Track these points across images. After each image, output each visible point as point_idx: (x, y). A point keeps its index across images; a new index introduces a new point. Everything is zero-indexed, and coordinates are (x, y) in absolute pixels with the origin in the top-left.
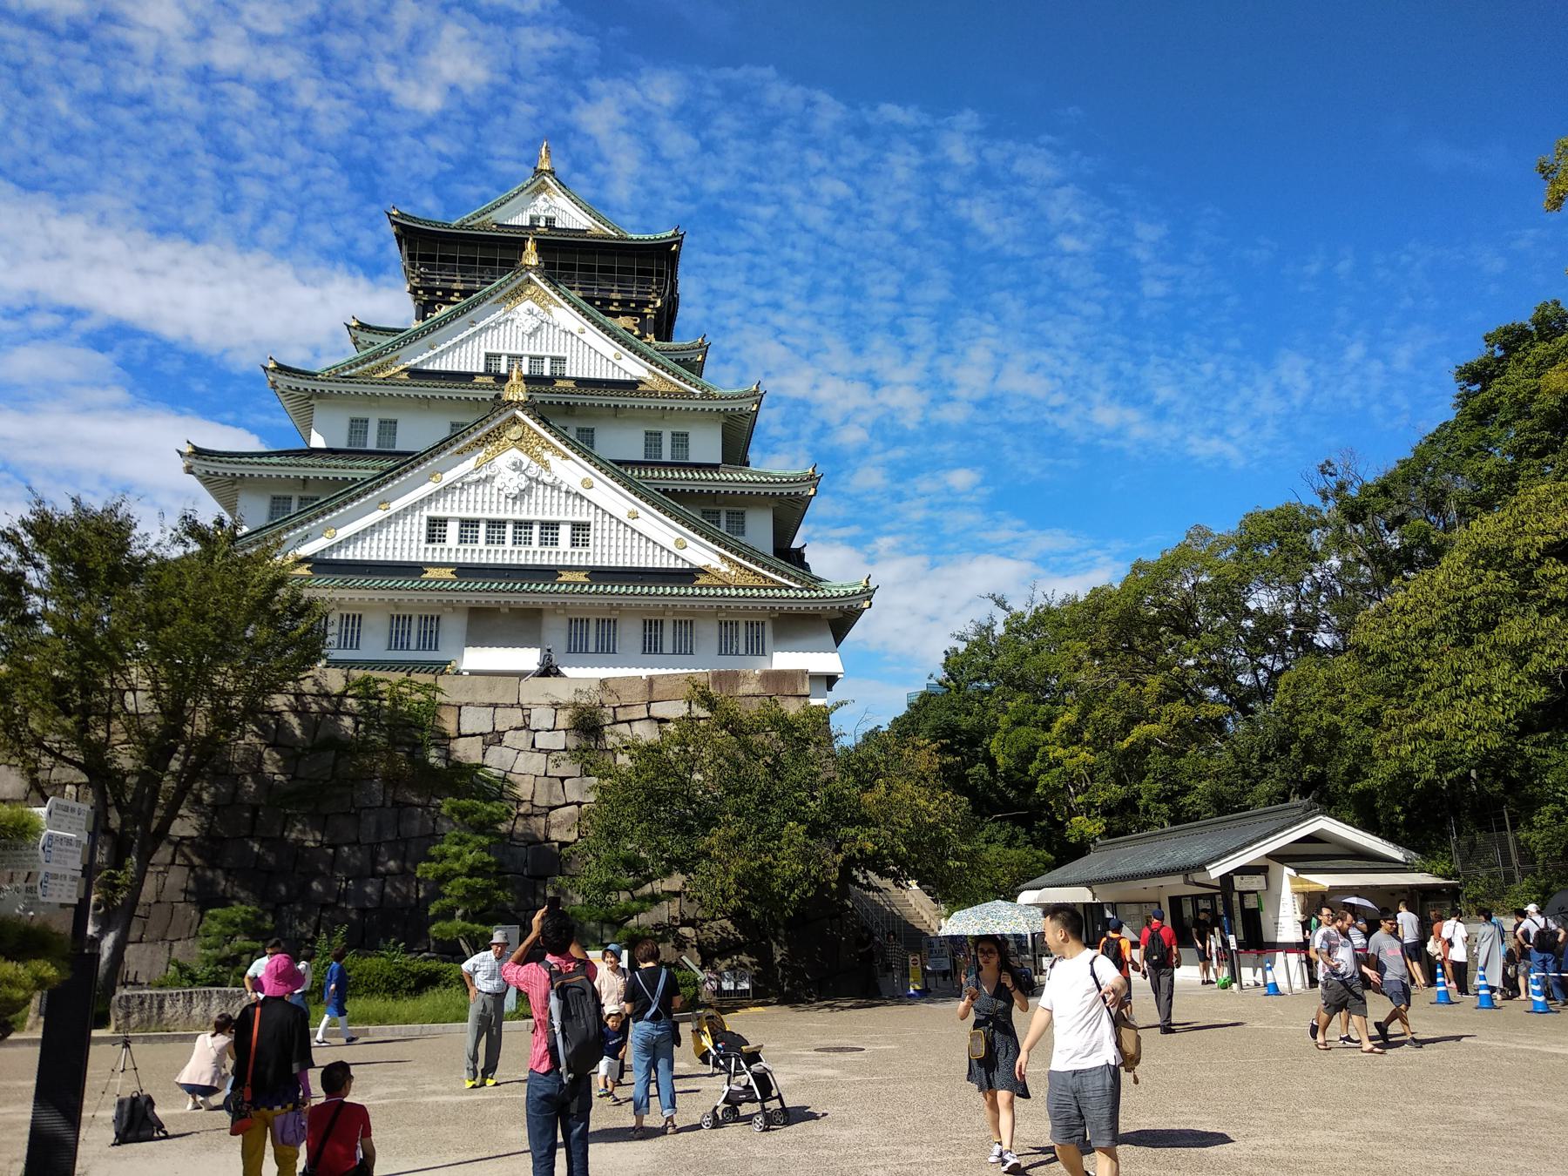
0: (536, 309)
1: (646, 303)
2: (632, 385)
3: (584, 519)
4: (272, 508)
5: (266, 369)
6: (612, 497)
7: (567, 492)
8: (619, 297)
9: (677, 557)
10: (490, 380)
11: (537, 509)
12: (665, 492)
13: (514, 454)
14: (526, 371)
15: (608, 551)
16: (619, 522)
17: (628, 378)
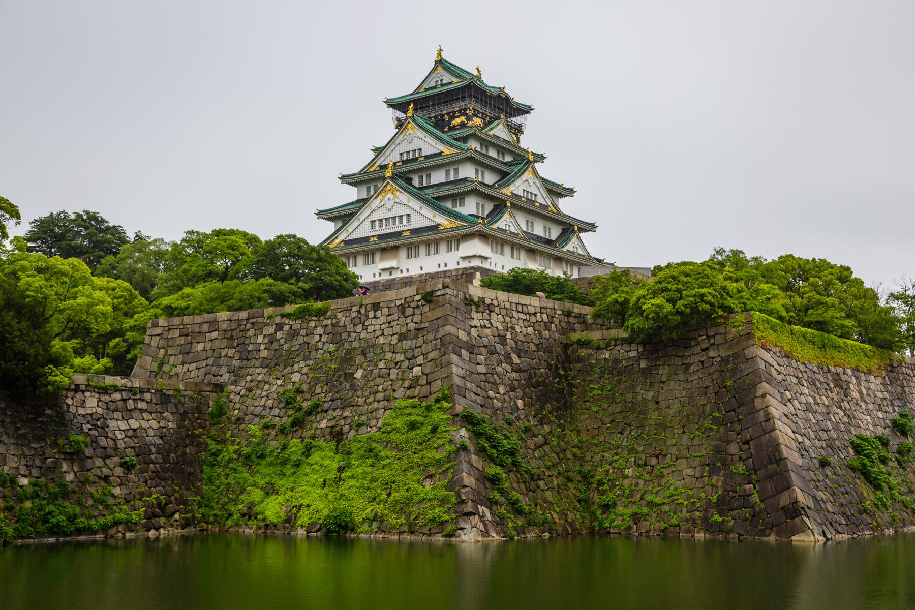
2: (440, 154)
6: (415, 204)
8: (457, 109)
11: (399, 211)
12: (433, 198)
13: (390, 195)
15: (418, 222)
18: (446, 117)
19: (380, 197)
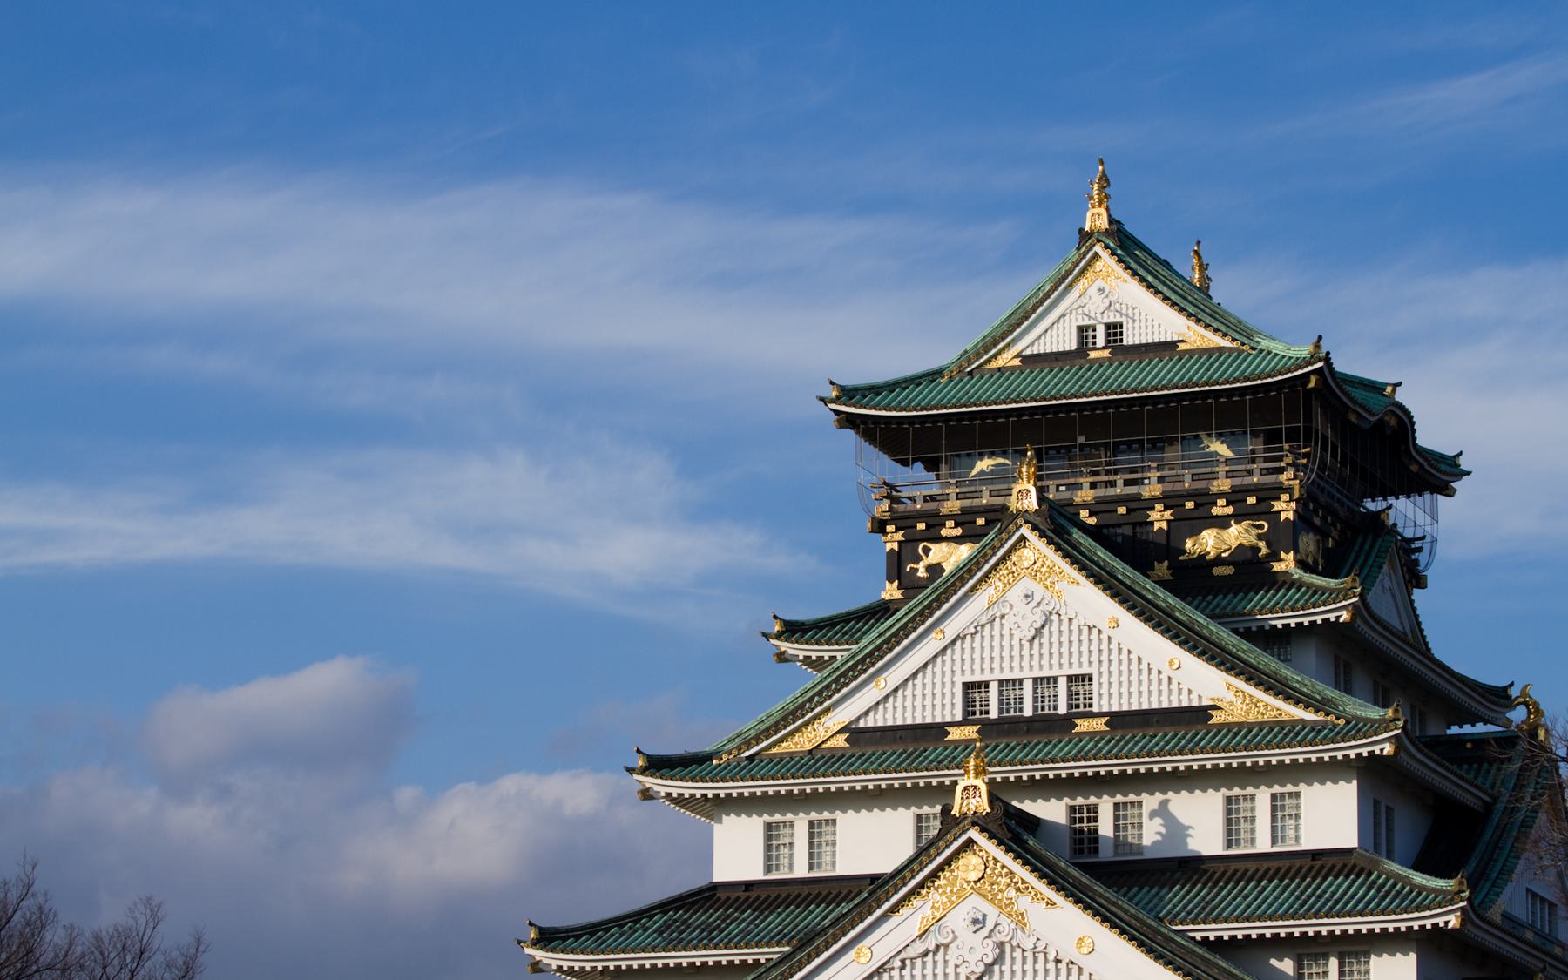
0: (1039, 591)
1: (1276, 491)
2: (1198, 715)
5: (630, 770)
10: (970, 732)
14: (1028, 712)
18: (1160, 518)
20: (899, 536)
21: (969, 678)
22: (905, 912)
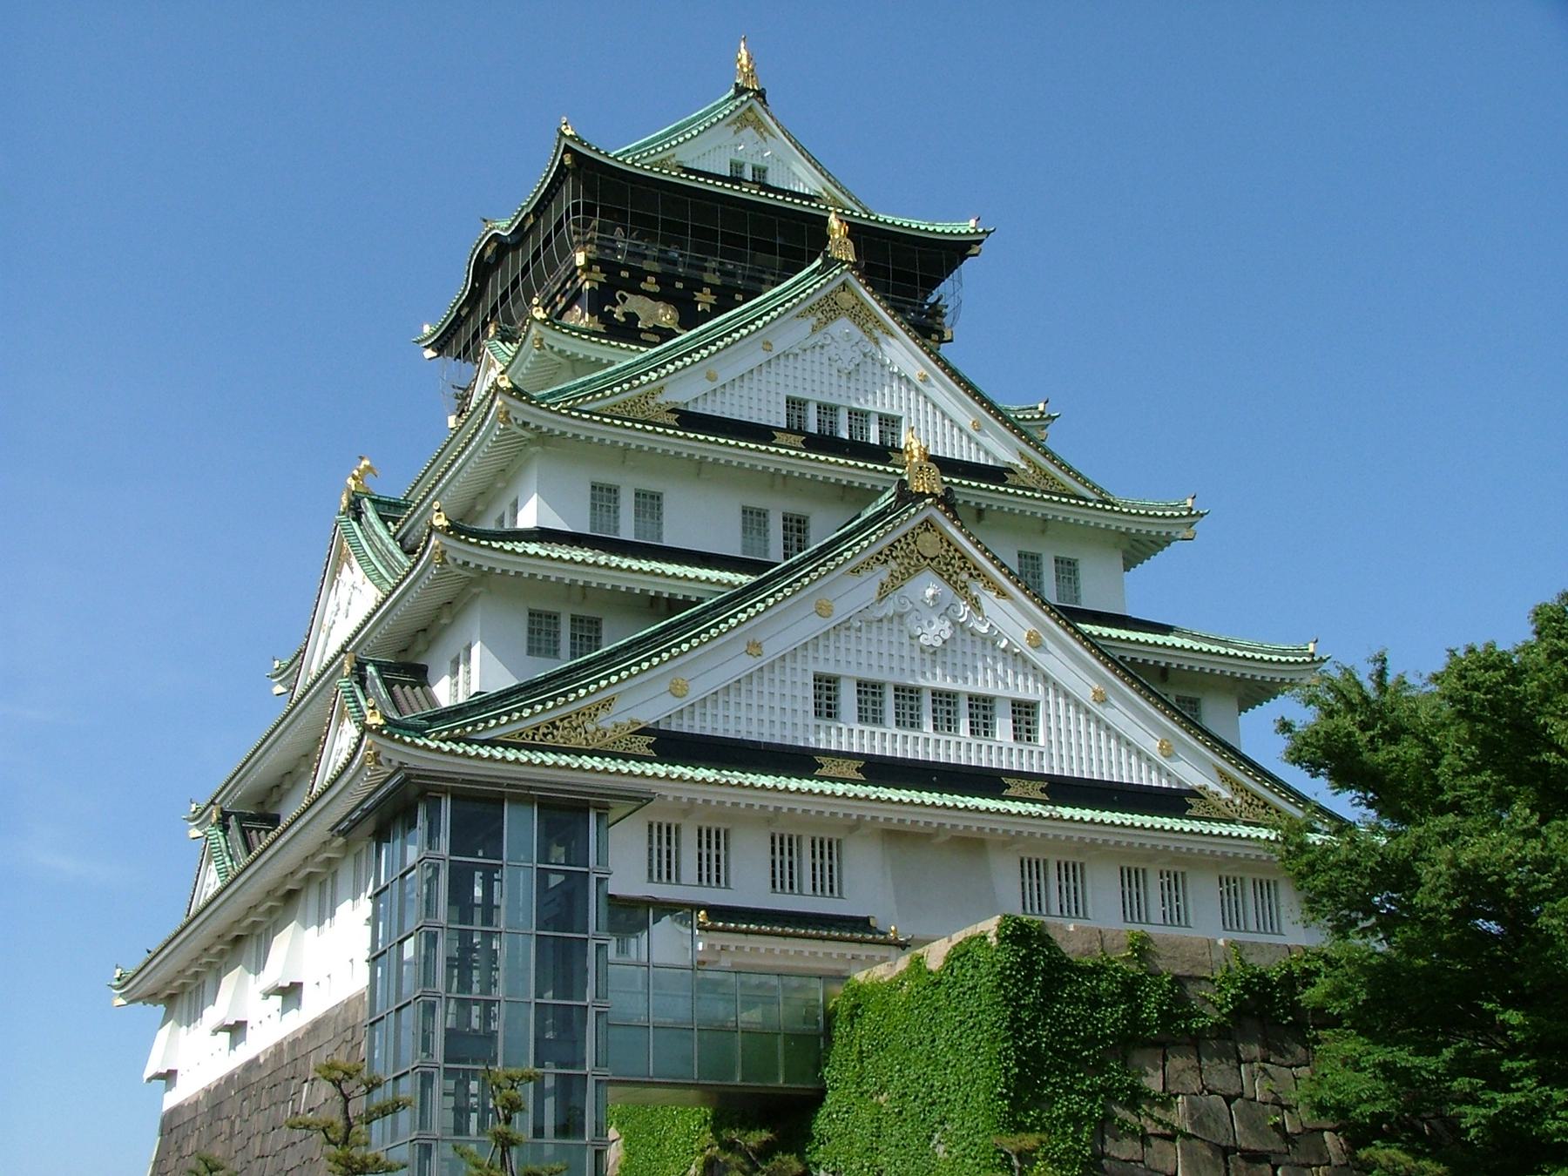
0: (858, 333)
3: (1030, 696)
4: (531, 631)
6: (1068, 665)
7: (1004, 650)
9: (1159, 768)
10: (798, 440)
16: (1078, 704)
17: (991, 463)
19: (882, 573)
20: (602, 278)
21: (793, 394)
22: (865, 574)
